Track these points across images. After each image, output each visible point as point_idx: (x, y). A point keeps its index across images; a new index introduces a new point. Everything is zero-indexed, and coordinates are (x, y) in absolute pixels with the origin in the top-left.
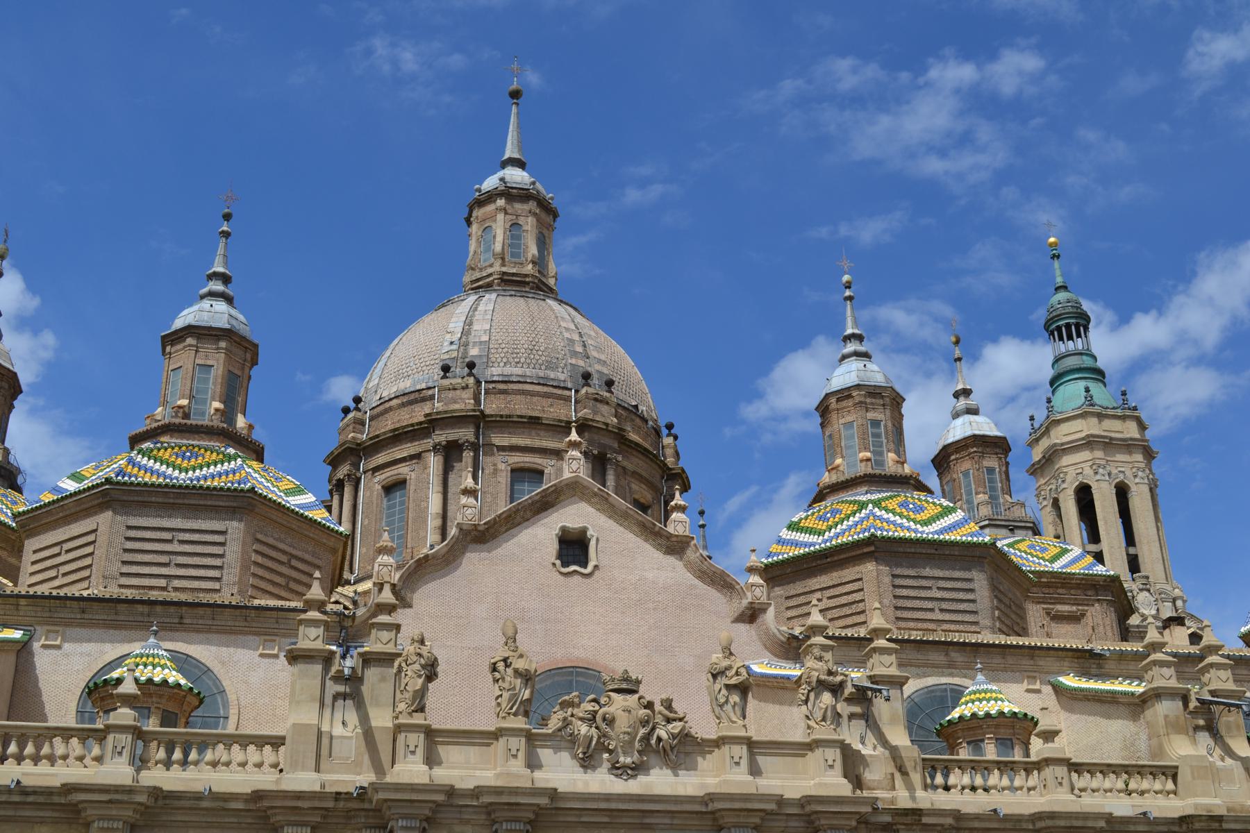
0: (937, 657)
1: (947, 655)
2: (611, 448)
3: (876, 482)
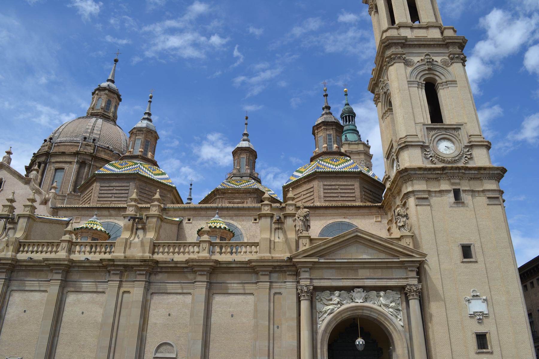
0: (106, 213)
1: (109, 212)
2: (88, 160)
3: (127, 158)
